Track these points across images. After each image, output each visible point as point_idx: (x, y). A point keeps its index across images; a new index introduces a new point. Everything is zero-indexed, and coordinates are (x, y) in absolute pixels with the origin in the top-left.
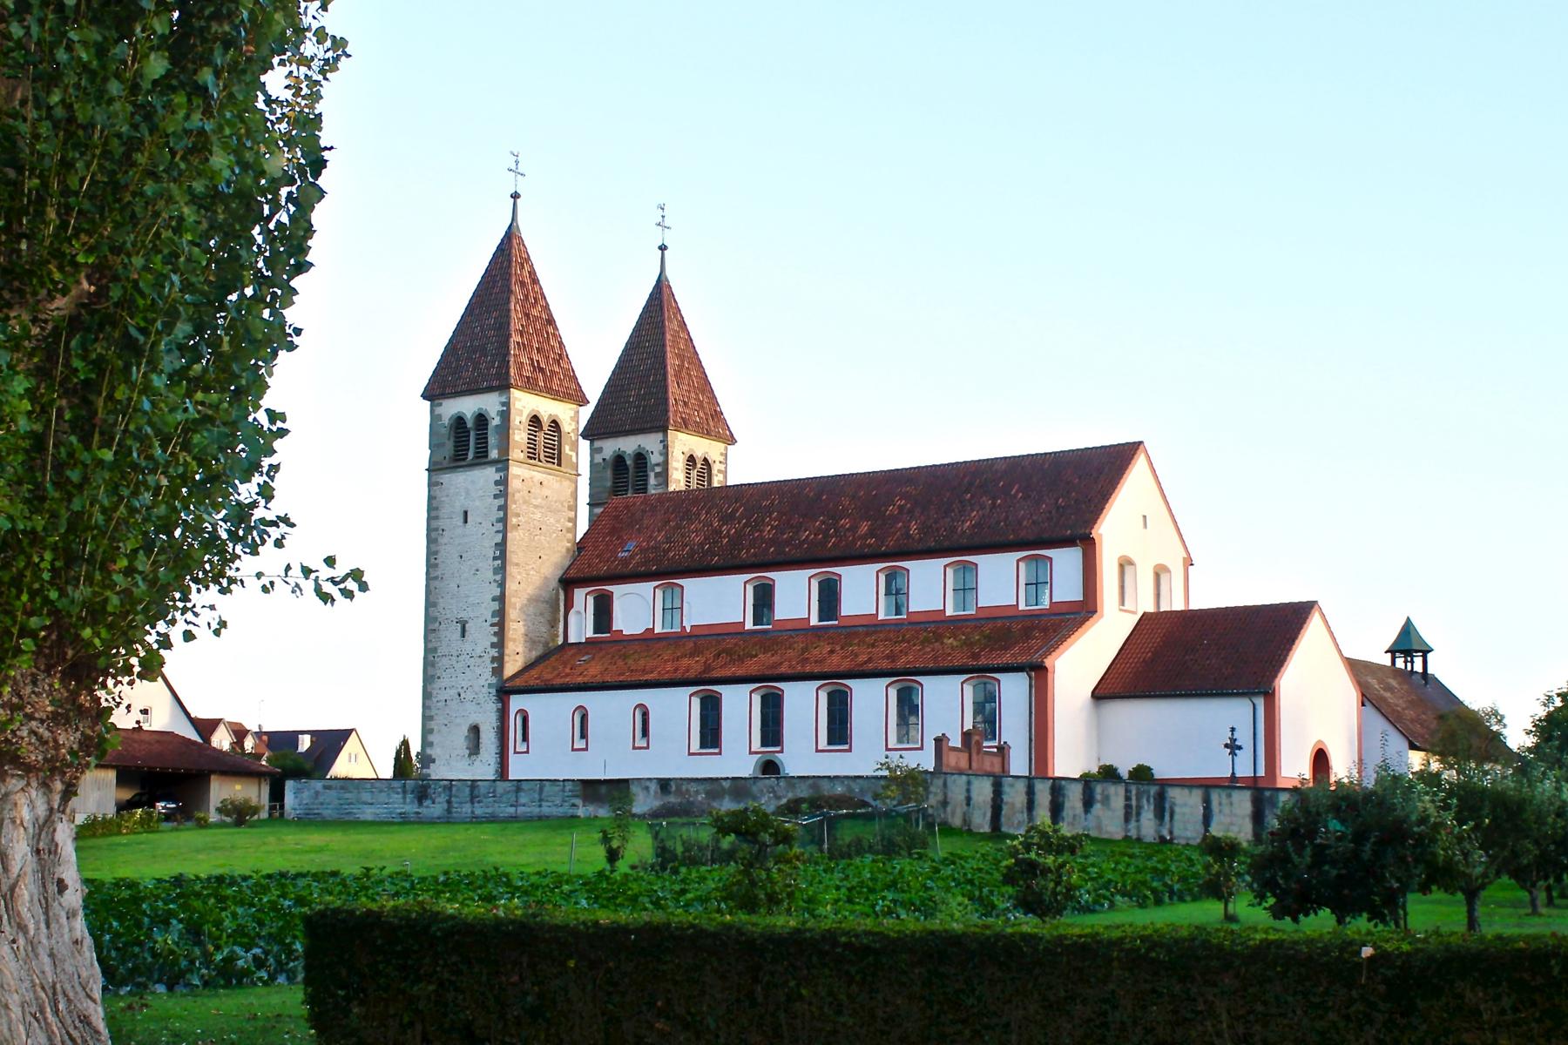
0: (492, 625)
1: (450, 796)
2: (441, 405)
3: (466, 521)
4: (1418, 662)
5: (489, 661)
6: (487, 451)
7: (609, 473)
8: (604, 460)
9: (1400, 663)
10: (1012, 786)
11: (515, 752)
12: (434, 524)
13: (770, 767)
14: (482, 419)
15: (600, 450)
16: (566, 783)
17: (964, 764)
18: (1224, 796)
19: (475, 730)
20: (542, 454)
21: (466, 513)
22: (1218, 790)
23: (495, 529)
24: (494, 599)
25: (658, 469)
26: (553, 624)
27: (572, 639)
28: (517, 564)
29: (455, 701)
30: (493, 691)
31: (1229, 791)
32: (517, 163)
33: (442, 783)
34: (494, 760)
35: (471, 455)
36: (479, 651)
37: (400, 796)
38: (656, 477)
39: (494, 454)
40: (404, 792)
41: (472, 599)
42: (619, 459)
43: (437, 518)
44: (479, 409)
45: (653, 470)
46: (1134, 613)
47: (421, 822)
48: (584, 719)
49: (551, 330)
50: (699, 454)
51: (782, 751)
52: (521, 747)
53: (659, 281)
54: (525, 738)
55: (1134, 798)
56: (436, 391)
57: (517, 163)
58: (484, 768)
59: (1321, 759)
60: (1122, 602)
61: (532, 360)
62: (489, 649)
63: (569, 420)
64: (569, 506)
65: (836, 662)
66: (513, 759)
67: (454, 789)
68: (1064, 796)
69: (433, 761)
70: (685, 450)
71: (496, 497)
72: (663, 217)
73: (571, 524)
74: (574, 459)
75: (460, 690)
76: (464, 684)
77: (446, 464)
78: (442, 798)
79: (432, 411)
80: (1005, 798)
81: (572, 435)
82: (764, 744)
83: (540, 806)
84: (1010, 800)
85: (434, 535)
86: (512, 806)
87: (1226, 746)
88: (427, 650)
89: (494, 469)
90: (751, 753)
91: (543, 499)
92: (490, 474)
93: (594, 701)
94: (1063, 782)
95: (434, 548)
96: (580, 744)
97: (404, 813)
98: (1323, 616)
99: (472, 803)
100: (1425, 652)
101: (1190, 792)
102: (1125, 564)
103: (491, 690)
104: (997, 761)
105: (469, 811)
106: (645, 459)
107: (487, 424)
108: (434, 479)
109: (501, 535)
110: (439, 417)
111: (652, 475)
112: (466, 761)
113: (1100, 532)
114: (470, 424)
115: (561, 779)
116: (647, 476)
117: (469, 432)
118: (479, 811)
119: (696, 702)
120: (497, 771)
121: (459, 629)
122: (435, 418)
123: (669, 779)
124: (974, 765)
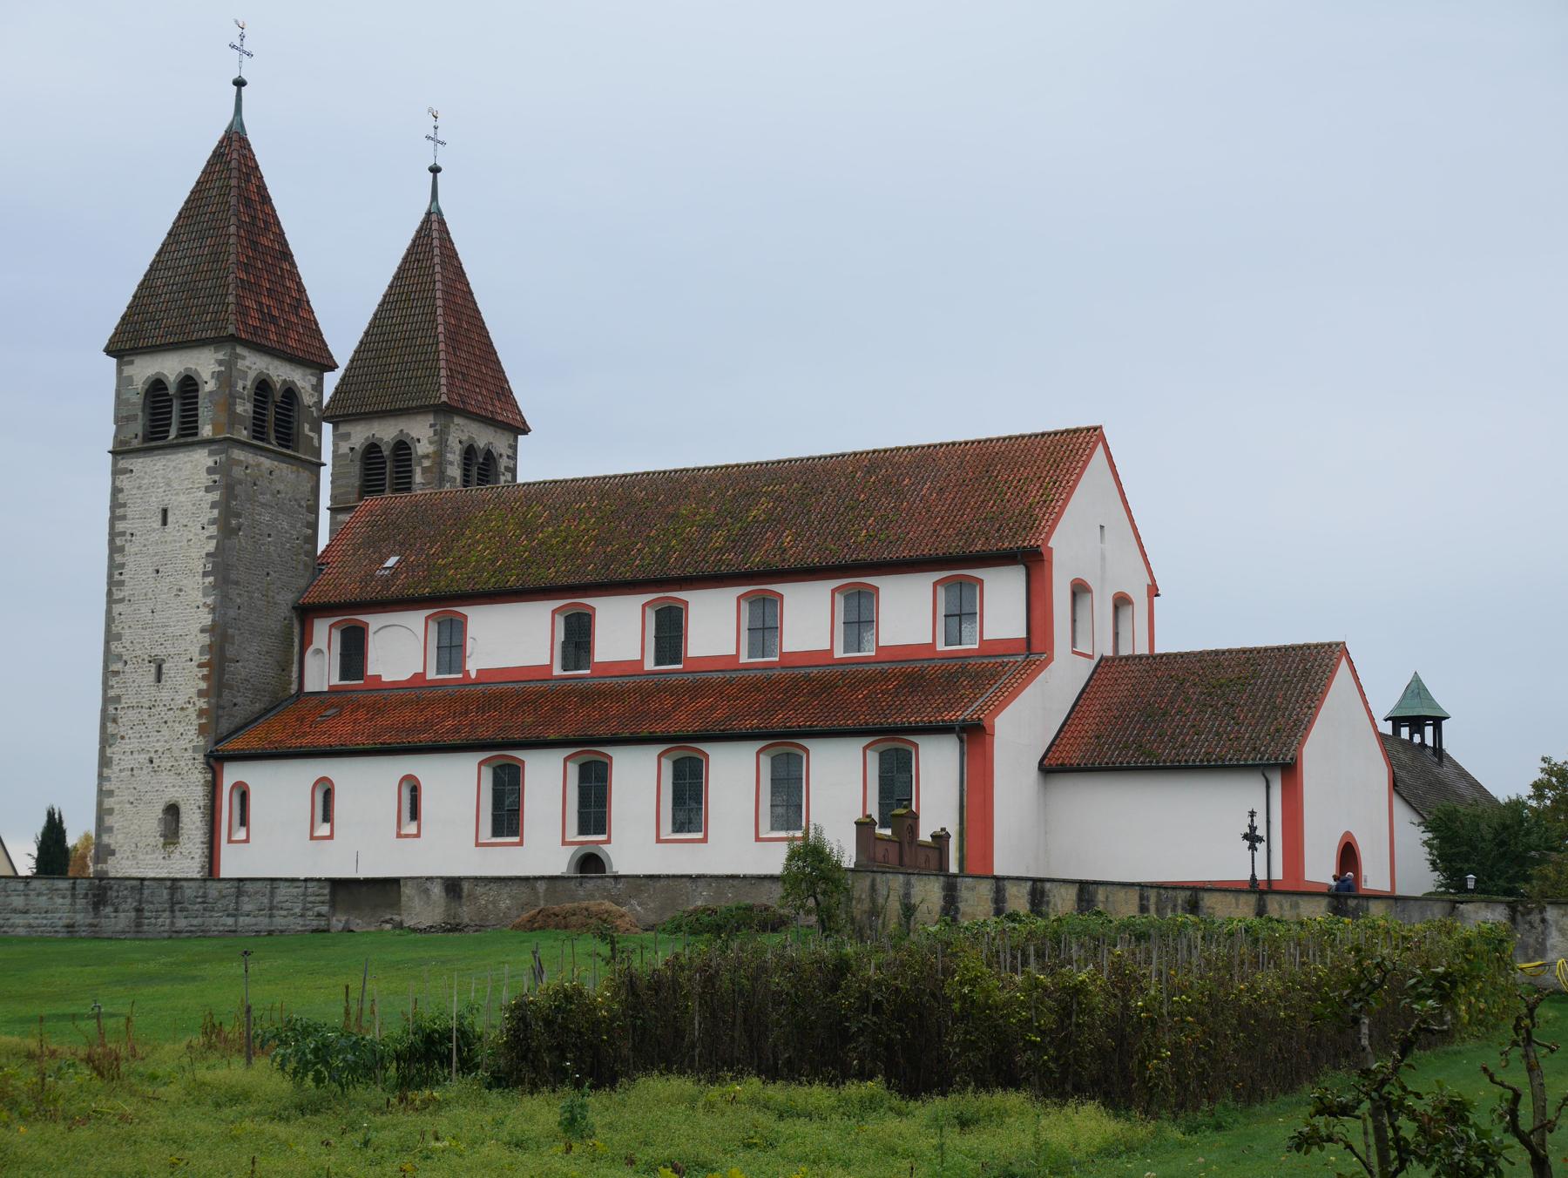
0: (200, 666)
1: (140, 902)
2: (132, 363)
3: (165, 523)
4: (1429, 731)
5: (194, 716)
6: (197, 428)
7: (356, 469)
8: (352, 449)
9: (1405, 733)
10: (973, 889)
11: (230, 841)
12: (120, 526)
13: (590, 863)
14: (189, 384)
15: (347, 436)
16: (309, 885)
17: (893, 857)
18: (1286, 906)
19: (173, 811)
20: (272, 435)
21: (165, 512)
22: (1278, 897)
23: (207, 533)
24: (203, 631)
25: (427, 463)
26: (284, 667)
27: (310, 687)
28: (237, 583)
29: (145, 772)
30: (200, 757)
31: (1295, 898)
32: (242, 37)
33: (127, 882)
34: (200, 851)
35: (173, 433)
36: (180, 700)
37: (68, 901)
38: (422, 474)
39: (206, 431)
40: (73, 896)
41: (170, 630)
42: (372, 449)
43: (124, 518)
44: (186, 369)
45: (420, 464)
46: (1091, 657)
47: (96, 934)
48: (328, 795)
49: (286, 266)
50: (481, 443)
51: (608, 841)
52: (241, 834)
53: (429, 213)
54: (244, 821)
55: (1152, 908)
56: (123, 347)
57: (242, 37)
58: (186, 862)
59: (1348, 855)
60: (1074, 644)
61: (261, 304)
62: (195, 699)
63: (309, 388)
64: (307, 506)
65: (682, 722)
66: (226, 850)
67: (146, 892)
68: (1048, 903)
69: (113, 853)
70: (464, 438)
71: (208, 490)
72: (436, 128)
73: (310, 531)
74: (316, 443)
75: (152, 755)
76: (158, 746)
77: (136, 443)
78: (131, 903)
79: (119, 371)
80: (962, 906)
81: (313, 409)
82: (583, 830)
83: (271, 916)
84: (969, 910)
85: (118, 542)
86: (228, 916)
87: (1246, 837)
88: (107, 700)
89: (206, 451)
90: (564, 843)
91: (273, 495)
93: (342, 772)
94: (1048, 886)
95: (118, 558)
96: (324, 830)
97: (73, 926)
98: (1350, 662)
99: (172, 911)
100: (1437, 722)
101: (1237, 900)
102: (1079, 590)
103: (196, 756)
104: (934, 855)
105: (168, 921)
106: (410, 449)
107: (197, 391)
108: (123, 464)
109: (215, 541)
110: (130, 380)
111: (418, 470)
112: (159, 854)
113: (1049, 545)
114: (172, 390)
115: (302, 877)
116: (410, 471)
117: (171, 400)
118: (181, 923)
119: (487, 775)
120: (203, 867)
121: (153, 670)
122: (123, 382)
123: (460, 879)
124: (906, 860)
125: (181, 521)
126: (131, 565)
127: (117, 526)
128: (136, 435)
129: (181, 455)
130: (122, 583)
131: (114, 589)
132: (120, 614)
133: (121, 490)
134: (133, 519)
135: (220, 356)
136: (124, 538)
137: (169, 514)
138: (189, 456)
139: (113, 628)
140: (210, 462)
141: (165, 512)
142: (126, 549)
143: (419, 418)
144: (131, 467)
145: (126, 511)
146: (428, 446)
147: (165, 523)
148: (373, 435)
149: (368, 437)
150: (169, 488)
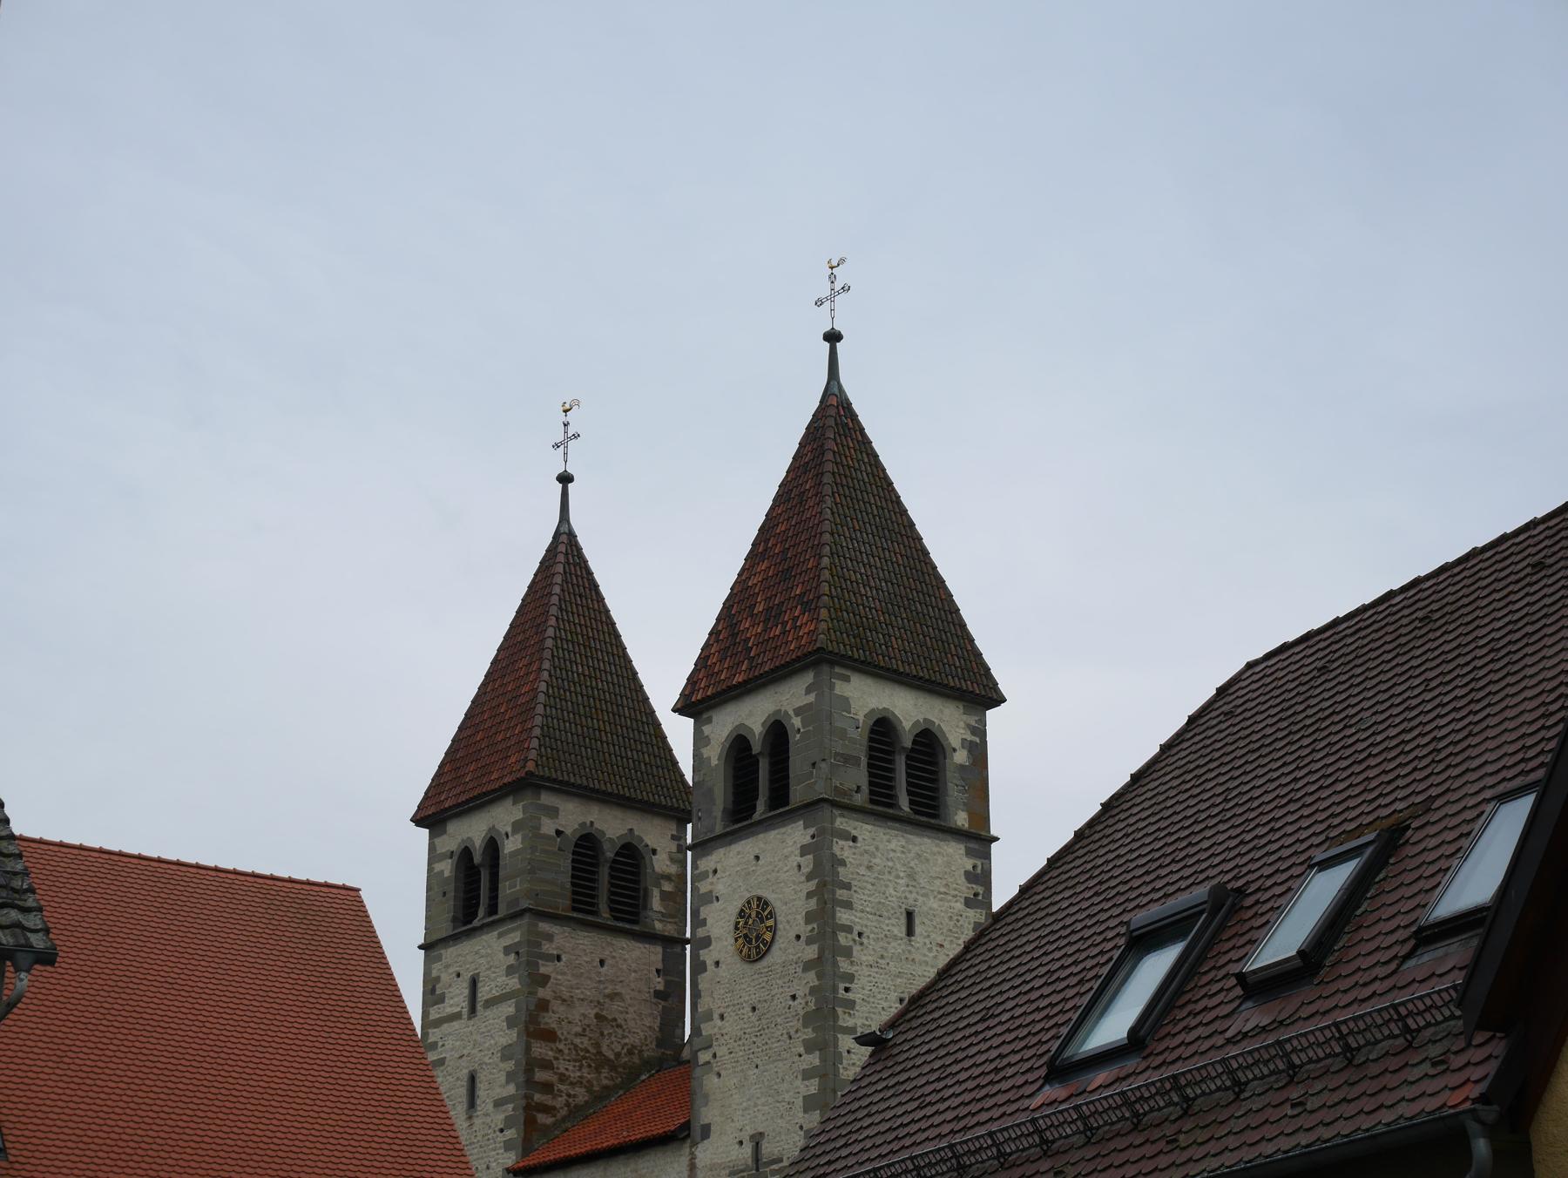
3: (910, 932)
8: (559, 833)
15: (553, 812)
21: (910, 916)
25: (667, 887)
38: (662, 900)
45: (658, 885)
92: (955, 855)
111: (656, 893)
125: (933, 936)
126: (864, 980)
127: (838, 915)
128: (859, 787)
129: (926, 840)
130: (851, 1004)
131: (840, 1010)
132: (849, 1052)
133: (843, 863)
134: (862, 911)
135: (972, 721)
136: (849, 936)
137: (917, 921)
138: (937, 846)
139: (841, 1071)
140: (968, 864)
141: (910, 916)
142: (855, 953)
143: (657, 821)
144: (854, 833)
145: (852, 897)
146: (668, 863)
147: (910, 932)
148: (592, 823)
149: (584, 823)
150: (914, 884)
